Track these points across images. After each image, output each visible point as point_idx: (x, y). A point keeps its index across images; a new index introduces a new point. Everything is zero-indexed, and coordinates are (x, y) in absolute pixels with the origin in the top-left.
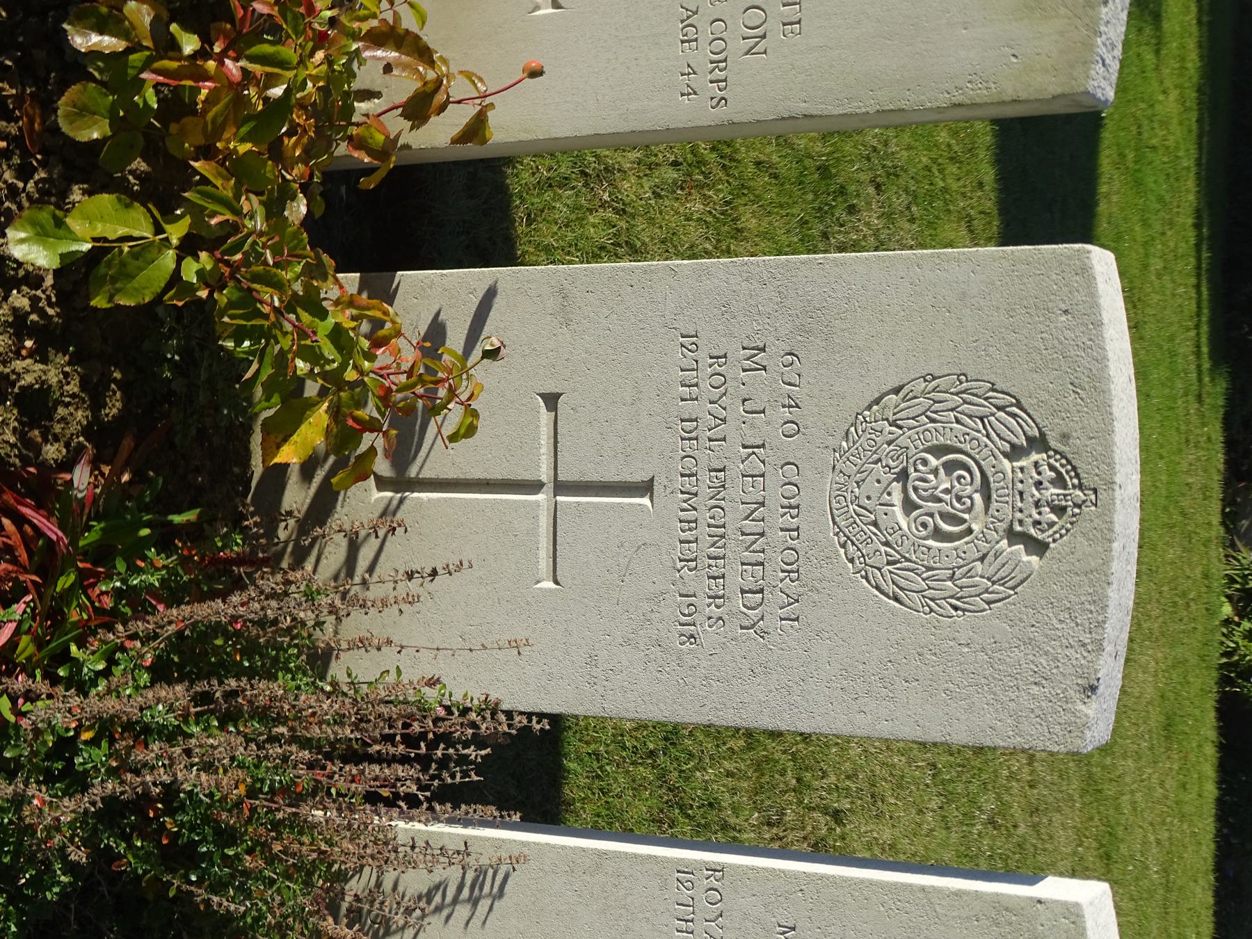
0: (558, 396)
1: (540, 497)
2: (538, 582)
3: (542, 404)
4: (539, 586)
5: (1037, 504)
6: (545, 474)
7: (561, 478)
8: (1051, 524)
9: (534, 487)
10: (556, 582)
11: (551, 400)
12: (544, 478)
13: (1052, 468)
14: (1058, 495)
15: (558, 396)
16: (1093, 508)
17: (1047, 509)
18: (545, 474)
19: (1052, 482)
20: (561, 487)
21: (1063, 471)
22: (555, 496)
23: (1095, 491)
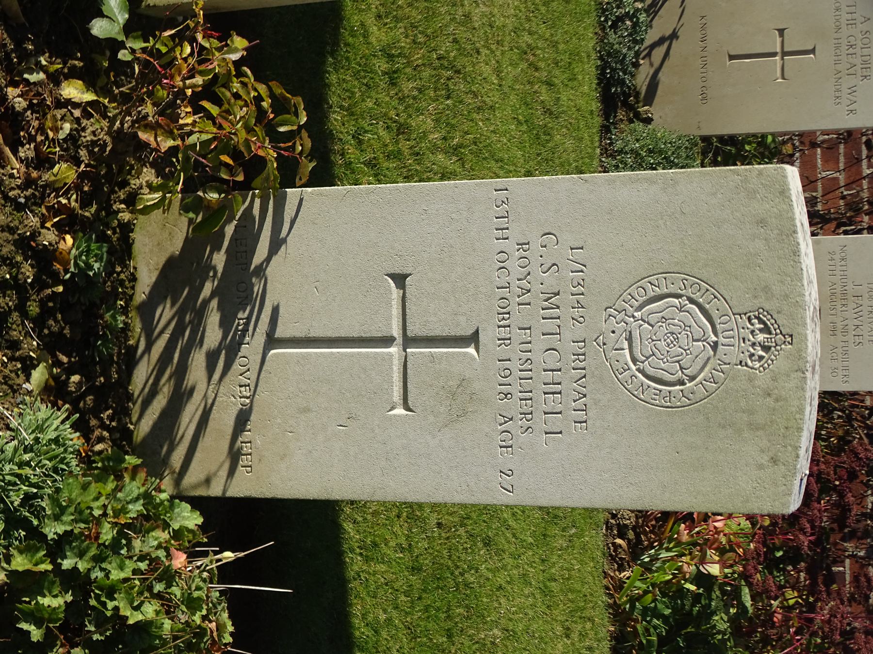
0: (406, 276)
1: (394, 349)
2: (392, 408)
3: (393, 284)
5: (754, 344)
6: (396, 332)
7: (409, 334)
8: (761, 358)
10: (408, 409)
11: (400, 279)
13: (761, 321)
14: (767, 338)
15: (406, 276)
17: (759, 348)
19: (761, 330)
20: (409, 341)
21: (768, 323)
22: (405, 350)
23: (791, 336)
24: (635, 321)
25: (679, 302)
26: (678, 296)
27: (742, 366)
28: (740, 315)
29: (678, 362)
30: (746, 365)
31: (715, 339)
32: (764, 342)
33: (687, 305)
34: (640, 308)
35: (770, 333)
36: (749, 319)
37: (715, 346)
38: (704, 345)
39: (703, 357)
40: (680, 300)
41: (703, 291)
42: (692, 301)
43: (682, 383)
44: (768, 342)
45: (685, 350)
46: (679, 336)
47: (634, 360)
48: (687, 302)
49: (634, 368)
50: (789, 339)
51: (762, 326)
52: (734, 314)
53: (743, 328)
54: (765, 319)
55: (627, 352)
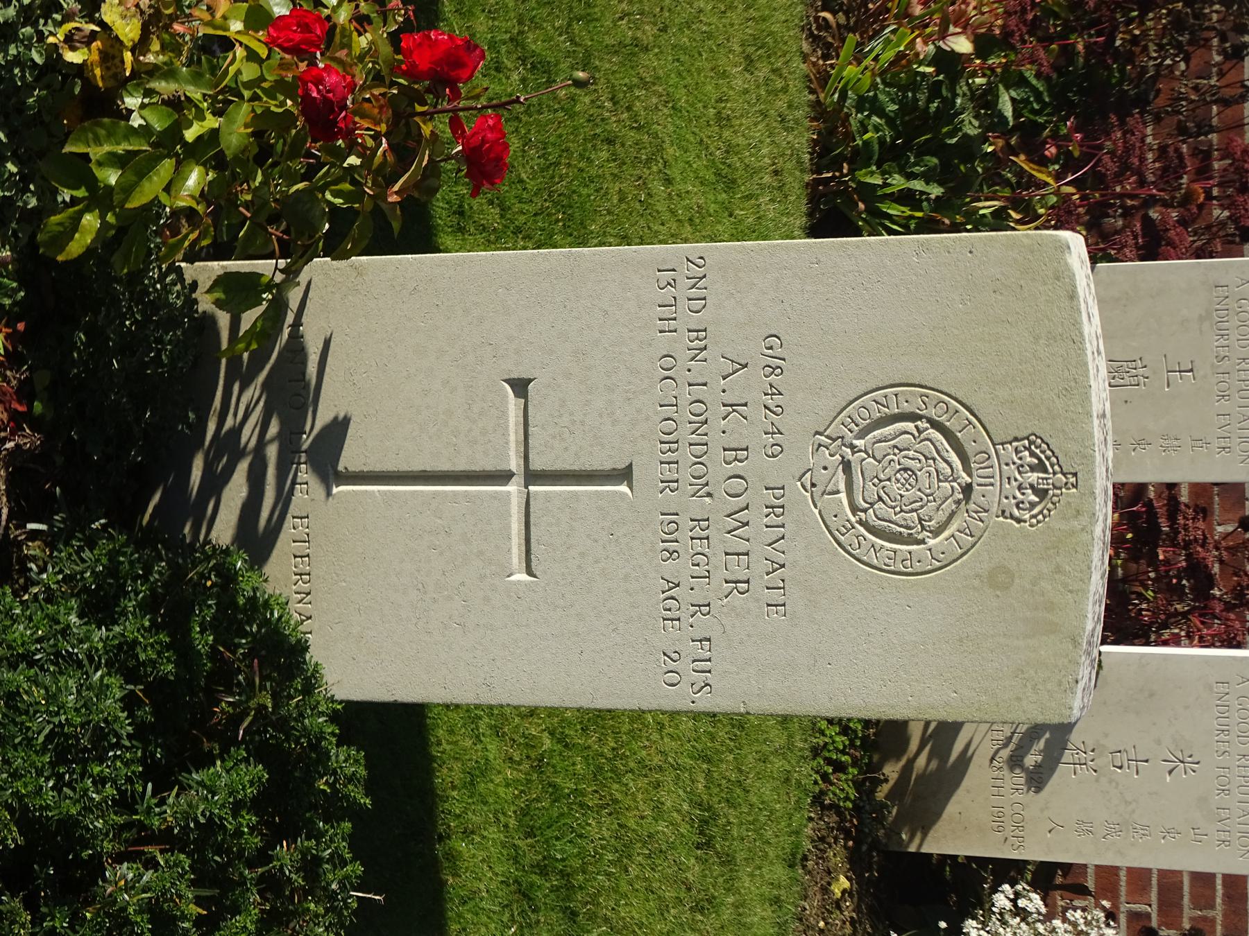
1: (513, 489)
4: (512, 578)
5: (1020, 488)
6: (514, 463)
7: (531, 467)
9: (503, 477)
10: (530, 572)
11: (520, 387)
12: (514, 469)
14: (1043, 479)
16: (1074, 490)
17: (1029, 491)
18: (514, 463)
19: (1033, 469)
20: (533, 477)
21: (1043, 456)
22: (526, 487)
23: (1075, 475)
25: (916, 427)
26: (913, 417)
27: (1006, 518)
28: (1002, 444)
30: (1012, 517)
32: (1038, 484)
33: (927, 429)
34: (862, 434)
35: (1046, 471)
36: (1017, 451)
37: (967, 490)
38: (952, 487)
39: (949, 505)
40: (919, 423)
41: (951, 411)
42: (935, 425)
43: (923, 542)
45: (927, 496)
46: (919, 473)
47: (854, 509)
48: (928, 425)
50: (1073, 480)
51: (1036, 461)
52: (994, 445)
53: (1007, 464)
54: (1038, 451)
55: (843, 496)
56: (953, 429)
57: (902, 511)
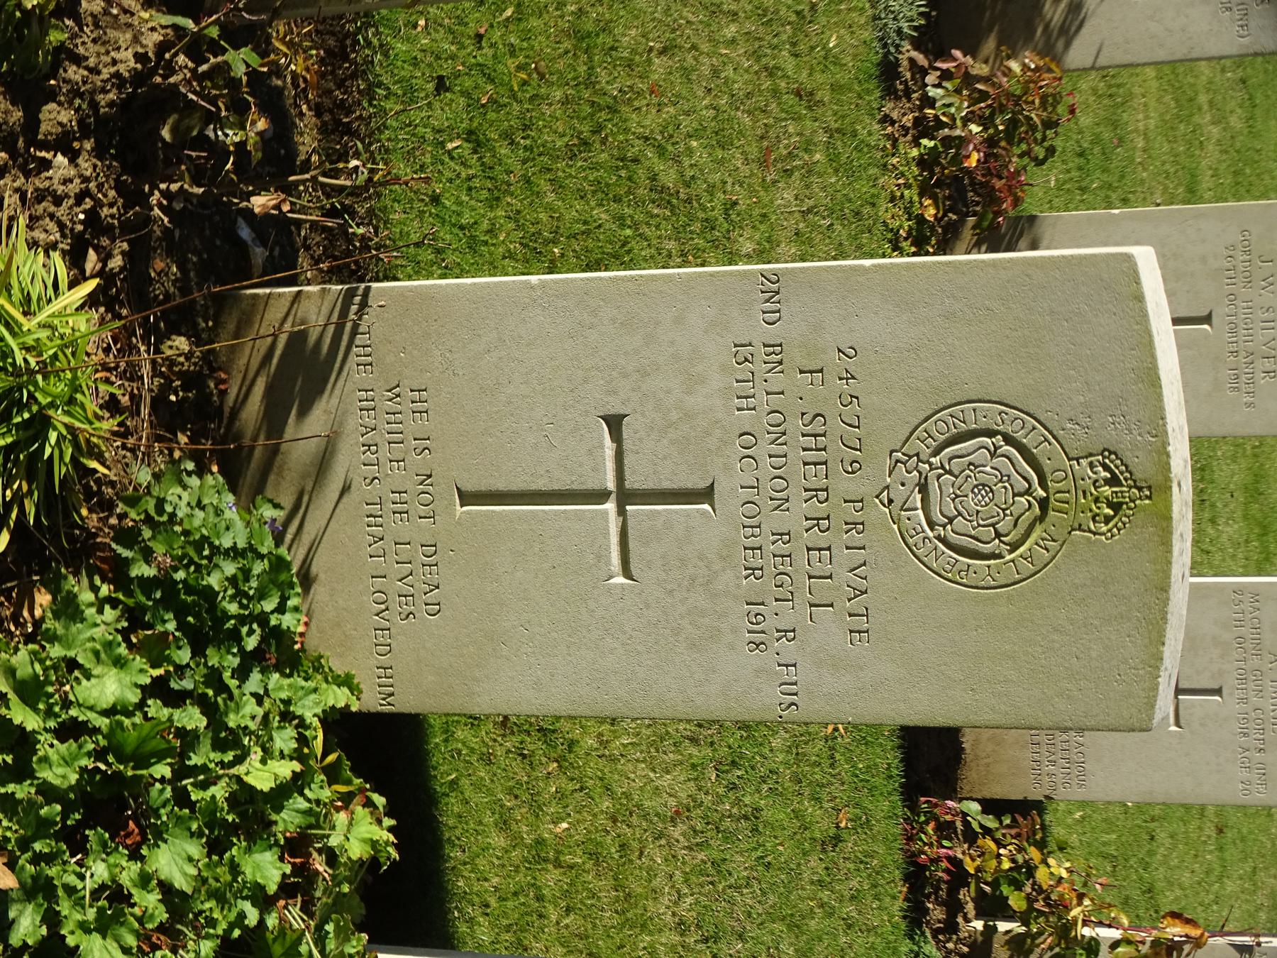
5: (1097, 500)
14: (1116, 492)
19: (1108, 482)
21: (1117, 471)
23: (1149, 488)
24: (931, 469)
26: (990, 433)
27: (1084, 531)
29: (993, 525)
30: (1090, 531)
31: (1042, 493)
33: (1001, 447)
36: (1091, 465)
37: (1044, 503)
38: (1028, 501)
42: (1008, 440)
43: (1000, 556)
44: (1117, 497)
45: (1004, 510)
46: (994, 488)
47: (932, 525)
48: (1003, 443)
49: (931, 534)
51: (1109, 475)
52: (1069, 459)
53: (1083, 479)
55: (920, 512)
56: (1030, 446)
57: (979, 525)
